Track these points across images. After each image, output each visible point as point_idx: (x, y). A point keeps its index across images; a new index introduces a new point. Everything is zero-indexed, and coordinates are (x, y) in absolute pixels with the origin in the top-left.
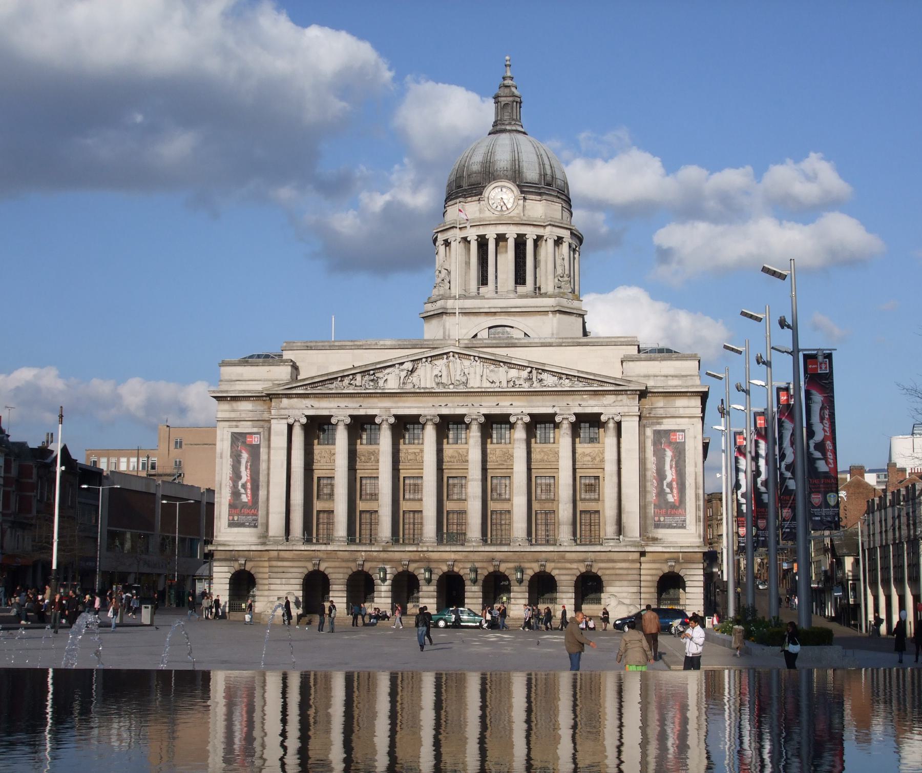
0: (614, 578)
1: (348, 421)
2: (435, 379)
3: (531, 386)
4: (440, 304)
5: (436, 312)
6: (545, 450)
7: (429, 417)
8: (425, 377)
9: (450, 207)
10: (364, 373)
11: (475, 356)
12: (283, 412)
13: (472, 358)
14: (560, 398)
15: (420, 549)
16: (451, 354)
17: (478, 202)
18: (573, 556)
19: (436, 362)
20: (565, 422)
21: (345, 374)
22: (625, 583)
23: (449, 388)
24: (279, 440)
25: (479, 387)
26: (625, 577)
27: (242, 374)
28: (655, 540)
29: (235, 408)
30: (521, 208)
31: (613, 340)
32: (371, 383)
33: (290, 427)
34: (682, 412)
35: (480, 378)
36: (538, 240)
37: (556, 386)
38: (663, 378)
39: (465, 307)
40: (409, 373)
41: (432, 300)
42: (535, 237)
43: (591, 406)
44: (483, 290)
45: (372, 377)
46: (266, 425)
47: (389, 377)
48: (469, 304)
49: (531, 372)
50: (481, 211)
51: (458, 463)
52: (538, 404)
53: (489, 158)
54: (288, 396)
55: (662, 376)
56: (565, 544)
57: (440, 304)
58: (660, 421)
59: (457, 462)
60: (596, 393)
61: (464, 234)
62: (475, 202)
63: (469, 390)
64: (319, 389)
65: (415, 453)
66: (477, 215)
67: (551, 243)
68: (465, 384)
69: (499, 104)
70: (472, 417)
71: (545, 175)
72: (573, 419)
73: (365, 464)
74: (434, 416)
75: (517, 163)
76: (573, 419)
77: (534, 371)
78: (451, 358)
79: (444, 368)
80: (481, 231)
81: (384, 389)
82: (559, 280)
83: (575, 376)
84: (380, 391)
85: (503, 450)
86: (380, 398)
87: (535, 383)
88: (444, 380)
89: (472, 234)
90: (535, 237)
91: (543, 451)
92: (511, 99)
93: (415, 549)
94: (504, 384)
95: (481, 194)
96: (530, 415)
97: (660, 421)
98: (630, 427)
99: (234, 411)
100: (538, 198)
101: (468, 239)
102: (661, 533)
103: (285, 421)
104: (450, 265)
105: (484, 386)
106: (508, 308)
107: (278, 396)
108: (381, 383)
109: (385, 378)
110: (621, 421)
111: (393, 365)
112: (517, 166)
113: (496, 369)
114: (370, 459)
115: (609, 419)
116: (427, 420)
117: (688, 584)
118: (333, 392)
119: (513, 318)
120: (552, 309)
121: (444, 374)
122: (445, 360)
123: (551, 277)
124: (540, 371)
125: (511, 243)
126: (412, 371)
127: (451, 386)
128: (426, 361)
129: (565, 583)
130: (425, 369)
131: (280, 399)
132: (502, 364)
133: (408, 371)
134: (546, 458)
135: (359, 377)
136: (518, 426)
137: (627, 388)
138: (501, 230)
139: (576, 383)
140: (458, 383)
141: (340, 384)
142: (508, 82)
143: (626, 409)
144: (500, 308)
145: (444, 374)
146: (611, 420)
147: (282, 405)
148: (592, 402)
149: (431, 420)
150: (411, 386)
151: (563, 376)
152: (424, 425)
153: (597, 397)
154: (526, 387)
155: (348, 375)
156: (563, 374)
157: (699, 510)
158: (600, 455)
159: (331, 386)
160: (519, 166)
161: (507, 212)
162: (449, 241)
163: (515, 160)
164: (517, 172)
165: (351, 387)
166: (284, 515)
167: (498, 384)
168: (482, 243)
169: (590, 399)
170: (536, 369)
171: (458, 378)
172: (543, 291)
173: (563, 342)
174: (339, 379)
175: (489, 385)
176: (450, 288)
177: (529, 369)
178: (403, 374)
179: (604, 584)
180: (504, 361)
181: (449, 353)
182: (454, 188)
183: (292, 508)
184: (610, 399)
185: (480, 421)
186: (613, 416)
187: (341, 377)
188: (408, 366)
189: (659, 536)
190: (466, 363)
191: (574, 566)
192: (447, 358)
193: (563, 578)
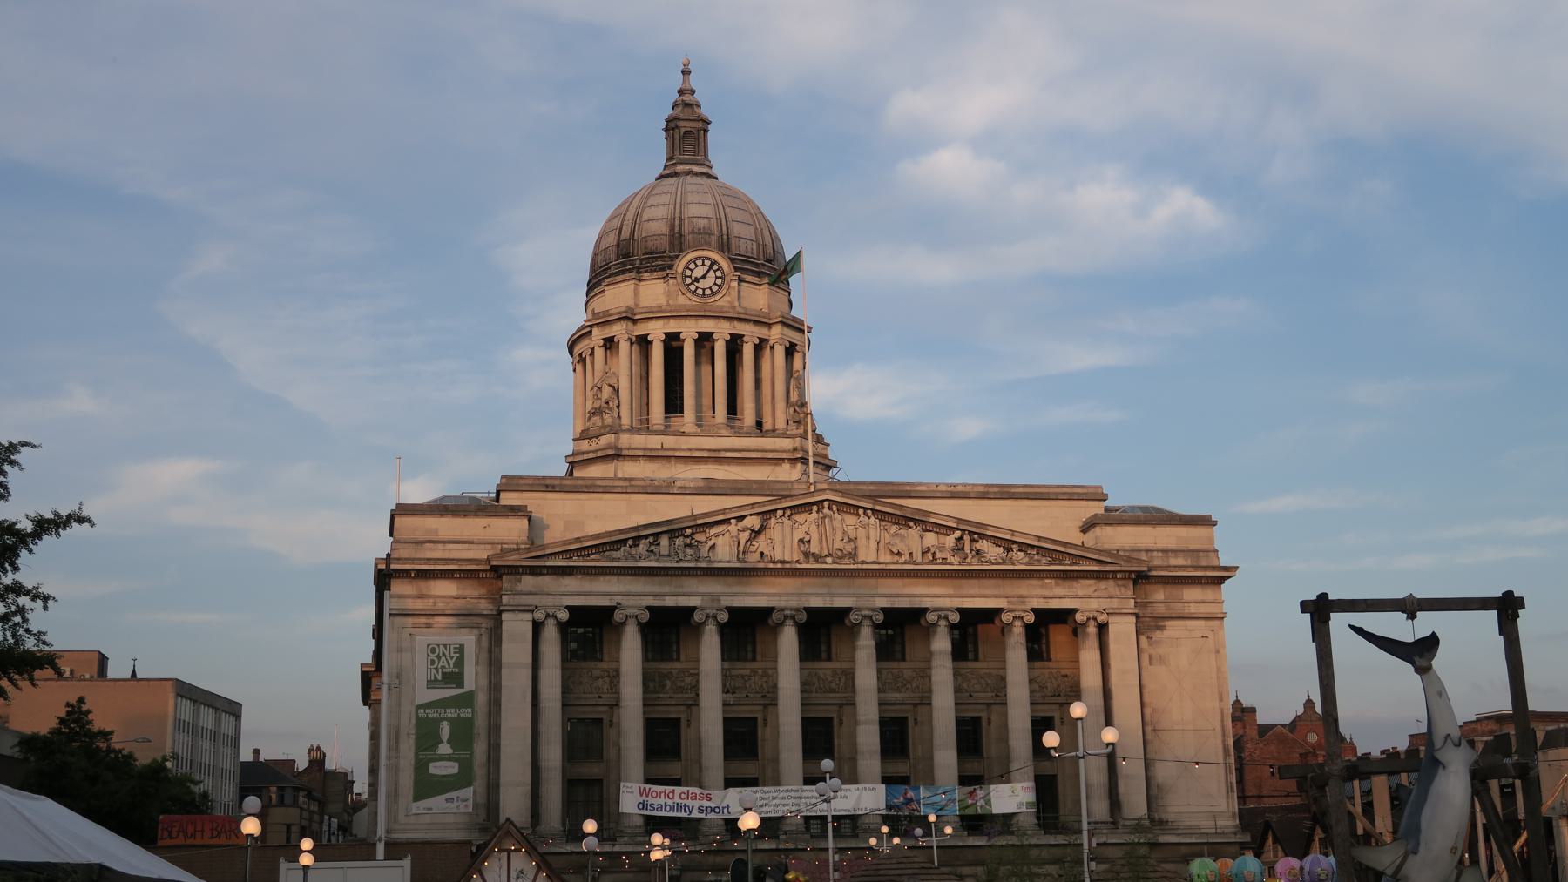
1: (645, 617)
3: (963, 562)
4: (604, 440)
5: (600, 454)
6: (963, 671)
7: (788, 612)
8: (783, 541)
9: (612, 287)
11: (865, 509)
13: (861, 511)
14: (1007, 582)
15: (781, 847)
16: (826, 504)
17: (662, 281)
18: (1045, 853)
19: (800, 518)
23: (826, 563)
24: (516, 651)
25: (874, 563)
27: (436, 531)
28: (1162, 823)
29: (425, 592)
30: (734, 293)
31: (1065, 490)
32: (689, 551)
33: (537, 627)
34: (1193, 609)
36: (759, 348)
37: (1004, 563)
38: (1160, 554)
39: (649, 446)
41: (591, 433)
42: (757, 341)
43: (1058, 597)
44: (675, 421)
45: (688, 541)
46: (485, 623)
47: (720, 541)
48: (654, 441)
50: (668, 295)
51: (818, 695)
52: (972, 592)
53: (678, 211)
54: (535, 571)
55: (1158, 551)
56: (1030, 832)
57: (604, 440)
58: (1161, 624)
59: (817, 692)
61: (640, 330)
62: (658, 281)
63: (860, 566)
64: (593, 560)
65: (743, 676)
66: (662, 301)
67: (780, 352)
68: (853, 555)
69: (677, 130)
70: (863, 613)
71: (764, 245)
72: (1030, 618)
73: (656, 696)
74: (797, 610)
76: (1030, 618)
77: (967, 537)
78: (826, 511)
79: (814, 528)
80: (673, 326)
82: (795, 411)
83: (1032, 547)
84: (704, 565)
85: (895, 671)
86: (701, 578)
87: (970, 556)
88: (814, 548)
89: (656, 331)
91: (961, 675)
94: (918, 557)
95: (671, 267)
96: (960, 610)
97: (1161, 624)
98: (1122, 631)
99: (421, 596)
100: (756, 280)
101: (650, 338)
103: (528, 616)
104: (618, 380)
105: (881, 560)
106: (719, 451)
107: (515, 571)
108: (704, 550)
109: (710, 543)
111: (727, 521)
114: (665, 686)
115: (1088, 619)
116: (786, 617)
118: (620, 564)
119: (726, 467)
120: (790, 456)
121: (815, 538)
122: (814, 515)
123: (781, 405)
124: (976, 536)
125: (720, 349)
126: (756, 533)
127: (829, 560)
131: (518, 577)
132: (911, 523)
133: (753, 531)
134: (965, 685)
135: (664, 541)
136: (939, 629)
137: (1118, 568)
138: (706, 326)
139: (1036, 557)
140: (839, 553)
141: (633, 550)
142: (687, 98)
143: (1115, 603)
144: (709, 450)
145: (815, 538)
146: (1092, 623)
147: (520, 587)
148: (1059, 591)
149: (793, 617)
150: (758, 557)
151: (1014, 546)
152: (782, 624)
153: (1068, 583)
154: (955, 563)
155: (646, 537)
156: (1016, 542)
157: (1231, 773)
158: (1054, 681)
159: (615, 554)
160: (727, 228)
161: (713, 299)
162: (616, 340)
163: (720, 218)
164: (725, 237)
165: (652, 557)
167: (907, 557)
168: (673, 345)
169: (1057, 584)
171: (839, 545)
172: (767, 426)
173: (988, 493)
174: (630, 542)
175: (888, 558)
176: (619, 416)
177: (958, 534)
178: (745, 536)
181: (824, 501)
182: (613, 256)
183: (544, 775)
184: (1085, 587)
185: (876, 620)
186: (1096, 614)
187: (633, 538)
188: (753, 522)
189: (1171, 817)
190: (851, 520)
192: (818, 512)
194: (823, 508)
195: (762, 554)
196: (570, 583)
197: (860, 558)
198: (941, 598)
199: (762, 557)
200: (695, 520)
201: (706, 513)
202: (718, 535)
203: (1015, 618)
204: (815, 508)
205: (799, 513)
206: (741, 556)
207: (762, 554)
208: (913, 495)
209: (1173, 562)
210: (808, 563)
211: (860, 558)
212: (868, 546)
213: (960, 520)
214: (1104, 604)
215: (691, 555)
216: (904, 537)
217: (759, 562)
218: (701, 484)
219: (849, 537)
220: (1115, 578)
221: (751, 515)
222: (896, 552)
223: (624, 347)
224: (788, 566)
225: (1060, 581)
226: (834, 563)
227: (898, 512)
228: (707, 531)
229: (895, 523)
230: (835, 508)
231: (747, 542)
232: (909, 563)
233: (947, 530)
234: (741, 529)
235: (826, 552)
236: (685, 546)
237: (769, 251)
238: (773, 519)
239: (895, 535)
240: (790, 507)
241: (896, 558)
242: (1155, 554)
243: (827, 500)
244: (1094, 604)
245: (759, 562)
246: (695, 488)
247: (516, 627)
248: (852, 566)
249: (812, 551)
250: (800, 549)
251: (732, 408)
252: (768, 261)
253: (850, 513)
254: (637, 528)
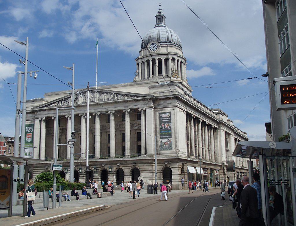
0: (143, 169)
10: (62, 100)
12: (38, 116)
13: (95, 92)
15: (78, 161)
18: (130, 162)
20: (126, 112)
21: (56, 101)
22: (148, 171)
26: (148, 169)
33: (40, 121)
36: (166, 60)
38: (163, 93)
43: (135, 106)
49: (114, 95)
54: (40, 111)
60: (137, 100)
67: (170, 60)
71: (169, 38)
75: (159, 35)
77: (115, 95)
80: (147, 59)
89: (145, 60)
90: (165, 59)
92: (160, 16)
93: (77, 162)
94: (106, 100)
96: (115, 110)
100: (166, 46)
102: (162, 152)
103: (38, 119)
110: (145, 110)
112: (159, 36)
115: (141, 110)
117: (173, 171)
125: (157, 62)
129: (126, 172)
135: (60, 103)
142: (160, 11)
147: (38, 114)
155: (57, 102)
166: (38, 151)
167: (104, 100)
168: (148, 62)
170: (116, 94)
174: (54, 103)
179: (140, 172)
184: (141, 102)
191: (130, 165)
193: (126, 170)
196: (46, 112)
198: (111, 109)
203: (126, 111)
208: (116, 87)
209: (166, 94)
213: (113, 91)
214: (145, 106)
220: (147, 100)
223: (140, 64)
225: (136, 102)
230: (90, 92)
233: (111, 94)
237: (170, 39)
242: (161, 93)
244: (143, 106)
247: (37, 122)
251: (160, 72)
252: (171, 41)
254: (54, 100)
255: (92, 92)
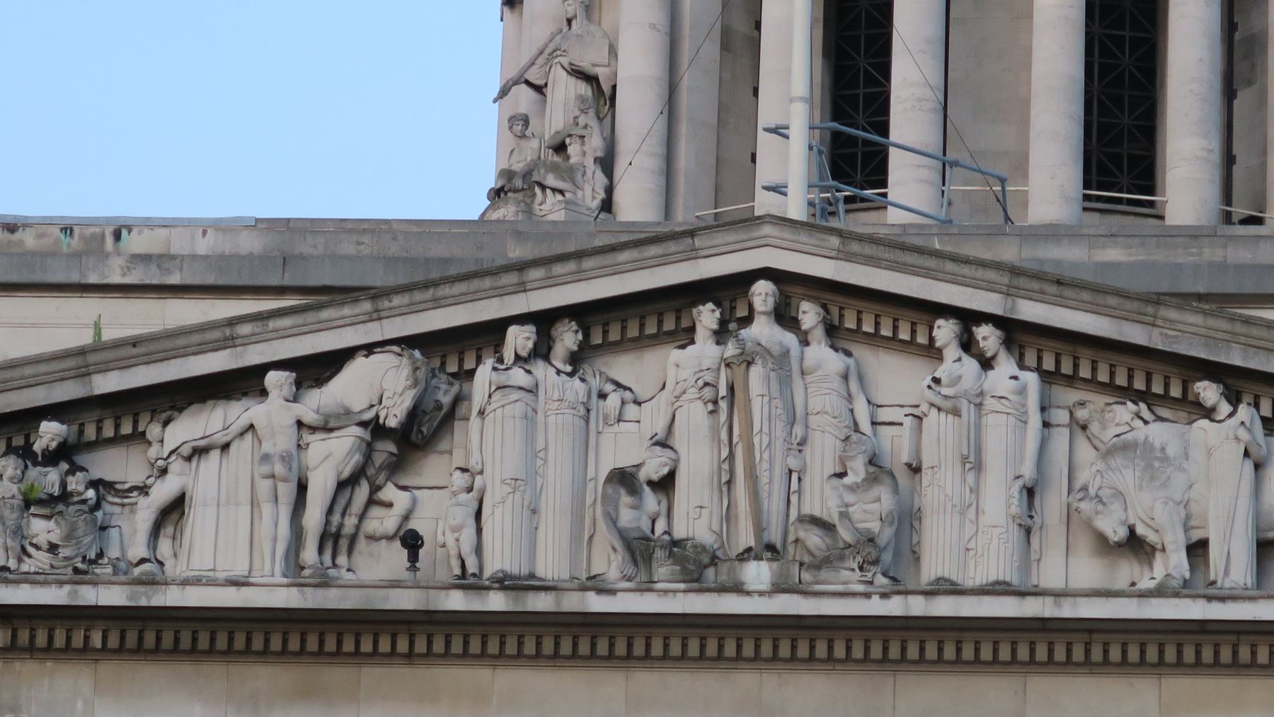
2: (610, 503)
11: (968, 318)
13: (945, 331)
16: (763, 293)
19: (624, 367)
23: (738, 588)
32: (42, 529)
35: (1016, 504)
40: (388, 447)
45: (50, 479)
63: (917, 606)
78: (763, 331)
79: (694, 416)
81: (149, 582)
84: (113, 596)
86: (109, 669)
105: (1051, 574)
109: (163, 492)
113: (1161, 434)
122: (705, 350)
127: (758, 573)
128: (542, 351)
130: (530, 419)
132: (1208, 392)
133: (376, 429)
140: (814, 539)
167: (1175, 563)
180: (1236, 358)
192: (721, 335)
194: (747, 321)
195: (412, 542)
197: (933, 567)
199: (413, 557)
200: (84, 374)
201: (135, 342)
202: (200, 452)
204: (707, 316)
205: (643, 342)
206: (309, 554)
207: (412, 542)
210: (647, 587)
211: (933, 567)
212: (971, 506)
215: (53, 548)
216: (1165, 459)
217: (395, 584)
218: (250, 244)
219: (872, 461)
221: (369, 349)
222: (1117, 533)
224: (541, 603)
226: (779, 588)
227: (1135, 334)
228: (154, 431)
229: (1127, 393)
230: (809, 314)
231: (345, 485)
232: (1184, 590)
234: (310, 417)
235: (745, 537)
236: (27, 503)
238: (485, 374)
239: (1124, 448)
240: (581, 313)
241: (1126, 572)
243: (767, 273)
245: (395, 584)
246: (218, 260)
248: (876, 607)
249: (679, 532)
250: (613, 520)
253: (893, 343)
255: (833, 331)
